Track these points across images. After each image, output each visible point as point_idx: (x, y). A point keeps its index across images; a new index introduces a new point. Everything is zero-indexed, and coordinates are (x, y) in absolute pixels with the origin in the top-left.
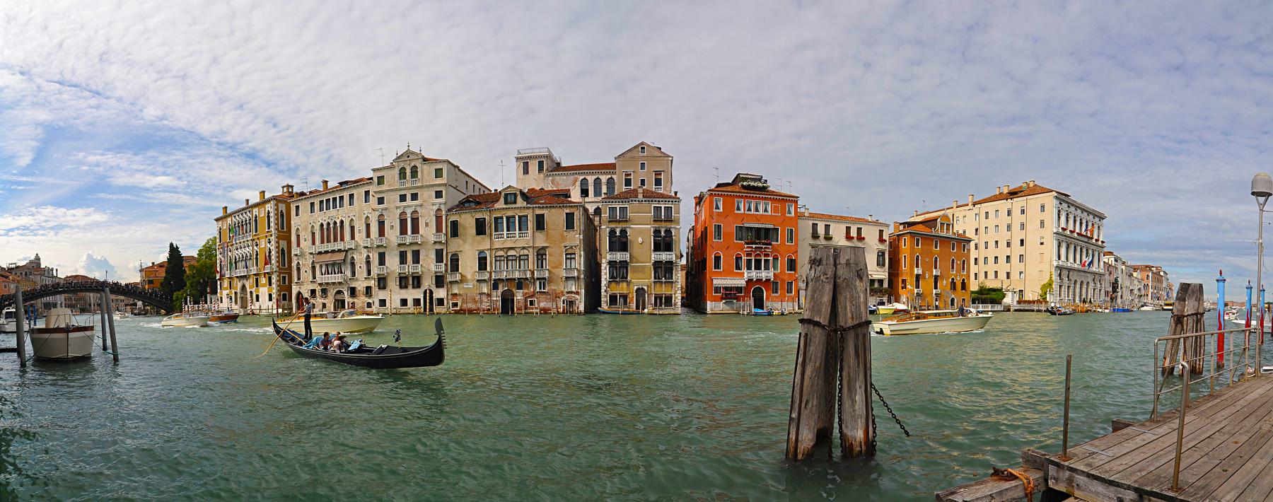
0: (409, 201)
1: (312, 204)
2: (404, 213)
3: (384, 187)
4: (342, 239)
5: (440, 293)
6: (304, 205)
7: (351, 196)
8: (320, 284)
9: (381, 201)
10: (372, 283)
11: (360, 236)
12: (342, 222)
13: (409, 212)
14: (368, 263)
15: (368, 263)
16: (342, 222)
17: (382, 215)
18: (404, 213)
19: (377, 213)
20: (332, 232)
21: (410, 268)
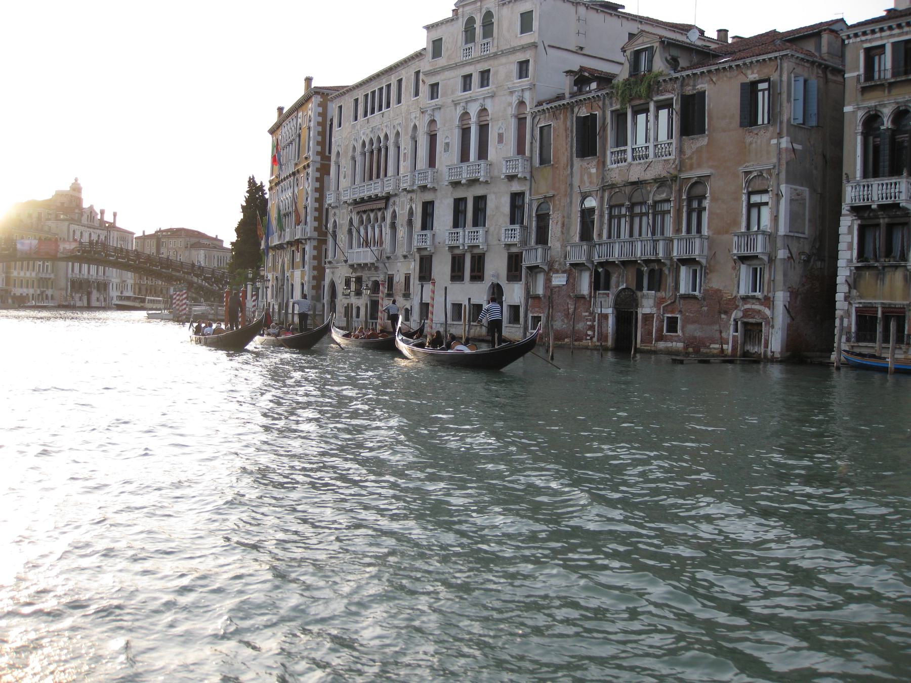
0: (476, 89)
1: (356, 100)
2: (465, 115)
3: (441, 62)
4: (386, 175)
5: (514, 294)
6: (348, 103)
7: (400, 81)
8: (352, 266)
9: (434, 87)
10: (413, 267)
11: (405, 166)
12: (386, 136)
13: (473, 110)
14: (410, 223)
15: (410, 223)
16: (386, 136)
17: (433, 122)
18: (465, 115)
19: (427, 118)
20: (375, 158)
21: (466, 237)
